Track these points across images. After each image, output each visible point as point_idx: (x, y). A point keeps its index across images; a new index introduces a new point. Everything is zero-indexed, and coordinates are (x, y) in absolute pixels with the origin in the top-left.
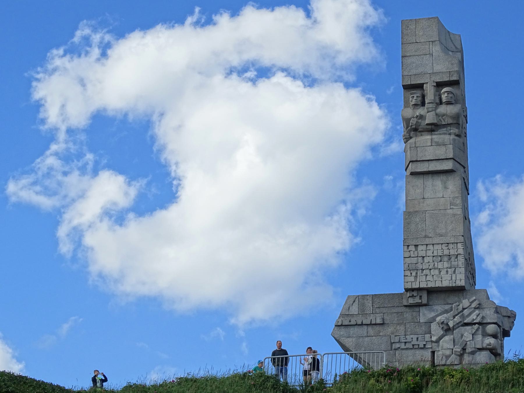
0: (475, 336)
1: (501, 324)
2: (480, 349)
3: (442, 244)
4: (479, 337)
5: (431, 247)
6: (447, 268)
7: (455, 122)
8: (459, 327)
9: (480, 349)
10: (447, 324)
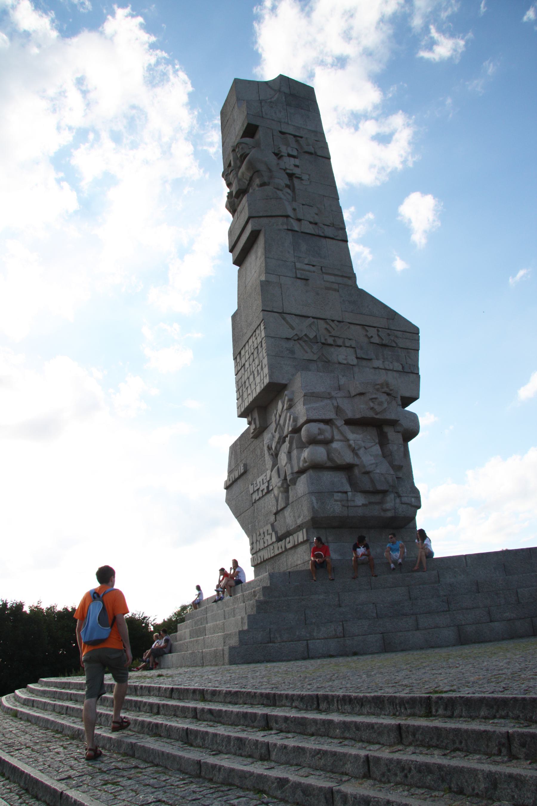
0: (292, 454)
1: (330, 415)
2: (301, 472)
3: (252, 335)
9: (301, 472)
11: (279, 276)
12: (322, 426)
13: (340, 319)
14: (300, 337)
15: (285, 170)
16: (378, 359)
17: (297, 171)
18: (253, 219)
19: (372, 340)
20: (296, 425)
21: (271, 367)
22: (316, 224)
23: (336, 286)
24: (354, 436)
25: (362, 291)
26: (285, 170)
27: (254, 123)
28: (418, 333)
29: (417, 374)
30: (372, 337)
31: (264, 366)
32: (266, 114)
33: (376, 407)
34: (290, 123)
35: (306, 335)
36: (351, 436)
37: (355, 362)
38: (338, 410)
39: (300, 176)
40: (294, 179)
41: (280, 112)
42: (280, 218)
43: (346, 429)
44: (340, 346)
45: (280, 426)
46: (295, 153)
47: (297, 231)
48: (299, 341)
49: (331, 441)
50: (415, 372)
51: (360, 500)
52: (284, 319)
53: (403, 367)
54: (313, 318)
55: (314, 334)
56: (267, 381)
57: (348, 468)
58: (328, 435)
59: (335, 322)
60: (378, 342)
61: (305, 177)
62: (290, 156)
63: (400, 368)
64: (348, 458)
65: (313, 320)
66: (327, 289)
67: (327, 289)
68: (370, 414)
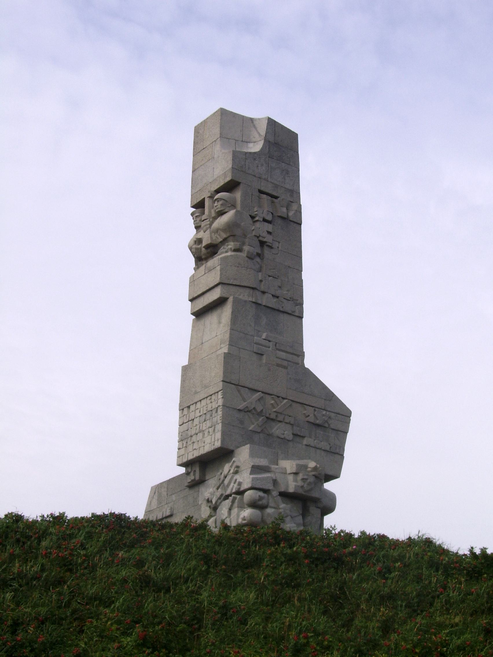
0: (232, 511)
1: (269, 486)
3: (207, 397)
4: (235, 511)
5: (199, 404)
6: (209, 428)
7: (228, 235)
8: (221, 503)
10: (211, 501)
11: (240, 348)
12: (261, 494)
13: (284, 397)
14: (250, 409)
15: (258, 237)
16: (310, 437)
17: (268, 239)
18: (223, 285)
20: (240, 488)
21: (223, 434)
22: (278, 297)
23: (285, 363)
24: (284, 506)
25: (308, 370)
26: (258, 237)
27: (237, 179)
28: (350, 417)
29: (342, 456)
30: (309, 416)
31: (216, 431)
32: (249, 168)
33: (305, 486)
34: (269, 179)
35: (254, 408)
36: (282, 506)
37: (291, 437)
38: (275, 482)
39: (270, 245)
40: (265, 246)
41: (262, 165)
42: (247, 289)
43: (279, 499)
44: (280, 422)
45: (224, 486)
46: (269, 218)
47: (260, 304)
48: (248, 413)
50: (341, 453)
52: (239, 391)
53: (331, 447)
54: (263, 392)
55: (262, 408)
56: (218, 444)
58: (264, 502)
59: (280, 398)
60: (312, 421)
61: (275, 245)
62: (265, 220)
63: (328, 448)
65: (262, 395)
66: (278, 365)
67: (278, 365)
68: (300, 491)
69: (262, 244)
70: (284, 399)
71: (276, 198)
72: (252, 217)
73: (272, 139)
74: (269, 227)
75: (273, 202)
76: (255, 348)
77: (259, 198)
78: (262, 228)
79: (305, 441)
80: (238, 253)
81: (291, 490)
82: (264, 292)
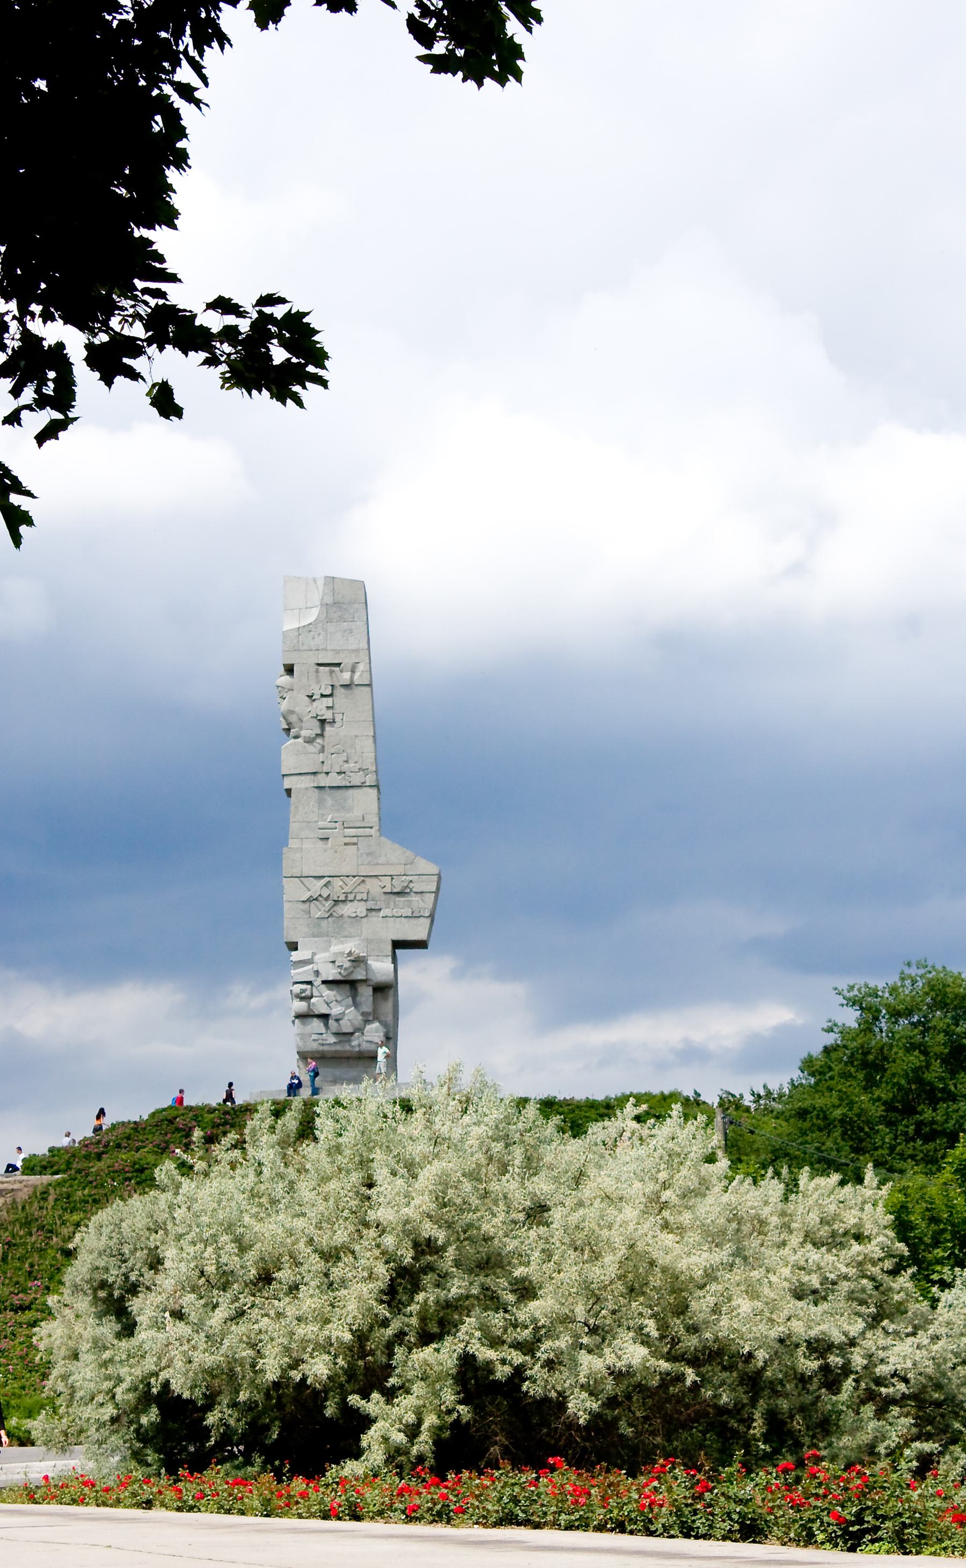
12: (304, 986)
17: (328, 715)
19: (386, 890)
23: (355, 840)
38: (317, 973)
43: (323, 987)
44: (351, 901)
46: (328, 692)
49: (312, 997)
51: (332, 1039)
57: (325, 1017)
58: (308, 993)
62: (322, 696)
64: (324, 1010)
65: (328, 879)
66: (346, 844)
67: (346, 844)
68: (339, 978)
69: (323, 722)
70: (354, 877)
71: (339, 665)
72: (310, 697)
73: (329, 600)
74: (328, 702)
75: (331, 672)
76: (322, 834)
77: (317, 671)
78: (320, 707)
79: (382, 914)
80: (296, 740)
81: (331, 978)
82: (327, 773)
